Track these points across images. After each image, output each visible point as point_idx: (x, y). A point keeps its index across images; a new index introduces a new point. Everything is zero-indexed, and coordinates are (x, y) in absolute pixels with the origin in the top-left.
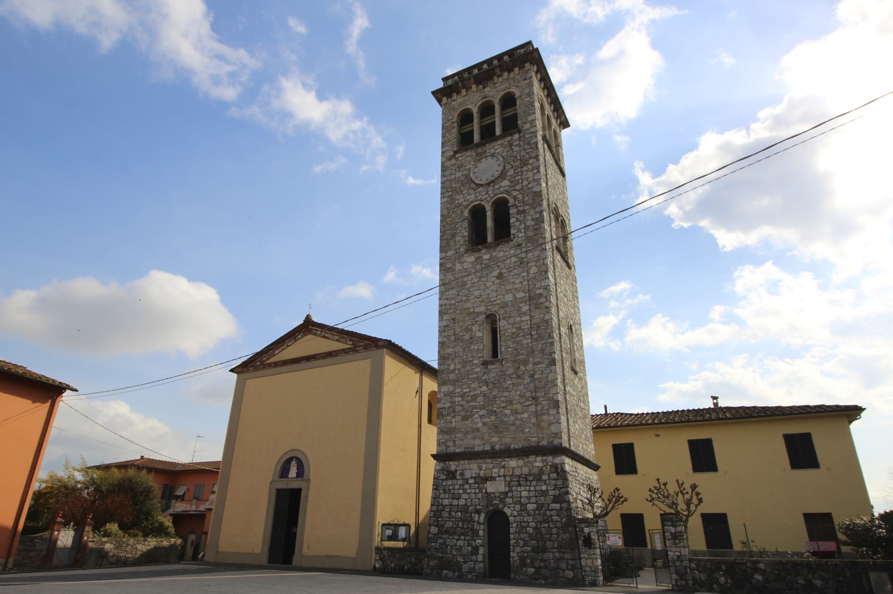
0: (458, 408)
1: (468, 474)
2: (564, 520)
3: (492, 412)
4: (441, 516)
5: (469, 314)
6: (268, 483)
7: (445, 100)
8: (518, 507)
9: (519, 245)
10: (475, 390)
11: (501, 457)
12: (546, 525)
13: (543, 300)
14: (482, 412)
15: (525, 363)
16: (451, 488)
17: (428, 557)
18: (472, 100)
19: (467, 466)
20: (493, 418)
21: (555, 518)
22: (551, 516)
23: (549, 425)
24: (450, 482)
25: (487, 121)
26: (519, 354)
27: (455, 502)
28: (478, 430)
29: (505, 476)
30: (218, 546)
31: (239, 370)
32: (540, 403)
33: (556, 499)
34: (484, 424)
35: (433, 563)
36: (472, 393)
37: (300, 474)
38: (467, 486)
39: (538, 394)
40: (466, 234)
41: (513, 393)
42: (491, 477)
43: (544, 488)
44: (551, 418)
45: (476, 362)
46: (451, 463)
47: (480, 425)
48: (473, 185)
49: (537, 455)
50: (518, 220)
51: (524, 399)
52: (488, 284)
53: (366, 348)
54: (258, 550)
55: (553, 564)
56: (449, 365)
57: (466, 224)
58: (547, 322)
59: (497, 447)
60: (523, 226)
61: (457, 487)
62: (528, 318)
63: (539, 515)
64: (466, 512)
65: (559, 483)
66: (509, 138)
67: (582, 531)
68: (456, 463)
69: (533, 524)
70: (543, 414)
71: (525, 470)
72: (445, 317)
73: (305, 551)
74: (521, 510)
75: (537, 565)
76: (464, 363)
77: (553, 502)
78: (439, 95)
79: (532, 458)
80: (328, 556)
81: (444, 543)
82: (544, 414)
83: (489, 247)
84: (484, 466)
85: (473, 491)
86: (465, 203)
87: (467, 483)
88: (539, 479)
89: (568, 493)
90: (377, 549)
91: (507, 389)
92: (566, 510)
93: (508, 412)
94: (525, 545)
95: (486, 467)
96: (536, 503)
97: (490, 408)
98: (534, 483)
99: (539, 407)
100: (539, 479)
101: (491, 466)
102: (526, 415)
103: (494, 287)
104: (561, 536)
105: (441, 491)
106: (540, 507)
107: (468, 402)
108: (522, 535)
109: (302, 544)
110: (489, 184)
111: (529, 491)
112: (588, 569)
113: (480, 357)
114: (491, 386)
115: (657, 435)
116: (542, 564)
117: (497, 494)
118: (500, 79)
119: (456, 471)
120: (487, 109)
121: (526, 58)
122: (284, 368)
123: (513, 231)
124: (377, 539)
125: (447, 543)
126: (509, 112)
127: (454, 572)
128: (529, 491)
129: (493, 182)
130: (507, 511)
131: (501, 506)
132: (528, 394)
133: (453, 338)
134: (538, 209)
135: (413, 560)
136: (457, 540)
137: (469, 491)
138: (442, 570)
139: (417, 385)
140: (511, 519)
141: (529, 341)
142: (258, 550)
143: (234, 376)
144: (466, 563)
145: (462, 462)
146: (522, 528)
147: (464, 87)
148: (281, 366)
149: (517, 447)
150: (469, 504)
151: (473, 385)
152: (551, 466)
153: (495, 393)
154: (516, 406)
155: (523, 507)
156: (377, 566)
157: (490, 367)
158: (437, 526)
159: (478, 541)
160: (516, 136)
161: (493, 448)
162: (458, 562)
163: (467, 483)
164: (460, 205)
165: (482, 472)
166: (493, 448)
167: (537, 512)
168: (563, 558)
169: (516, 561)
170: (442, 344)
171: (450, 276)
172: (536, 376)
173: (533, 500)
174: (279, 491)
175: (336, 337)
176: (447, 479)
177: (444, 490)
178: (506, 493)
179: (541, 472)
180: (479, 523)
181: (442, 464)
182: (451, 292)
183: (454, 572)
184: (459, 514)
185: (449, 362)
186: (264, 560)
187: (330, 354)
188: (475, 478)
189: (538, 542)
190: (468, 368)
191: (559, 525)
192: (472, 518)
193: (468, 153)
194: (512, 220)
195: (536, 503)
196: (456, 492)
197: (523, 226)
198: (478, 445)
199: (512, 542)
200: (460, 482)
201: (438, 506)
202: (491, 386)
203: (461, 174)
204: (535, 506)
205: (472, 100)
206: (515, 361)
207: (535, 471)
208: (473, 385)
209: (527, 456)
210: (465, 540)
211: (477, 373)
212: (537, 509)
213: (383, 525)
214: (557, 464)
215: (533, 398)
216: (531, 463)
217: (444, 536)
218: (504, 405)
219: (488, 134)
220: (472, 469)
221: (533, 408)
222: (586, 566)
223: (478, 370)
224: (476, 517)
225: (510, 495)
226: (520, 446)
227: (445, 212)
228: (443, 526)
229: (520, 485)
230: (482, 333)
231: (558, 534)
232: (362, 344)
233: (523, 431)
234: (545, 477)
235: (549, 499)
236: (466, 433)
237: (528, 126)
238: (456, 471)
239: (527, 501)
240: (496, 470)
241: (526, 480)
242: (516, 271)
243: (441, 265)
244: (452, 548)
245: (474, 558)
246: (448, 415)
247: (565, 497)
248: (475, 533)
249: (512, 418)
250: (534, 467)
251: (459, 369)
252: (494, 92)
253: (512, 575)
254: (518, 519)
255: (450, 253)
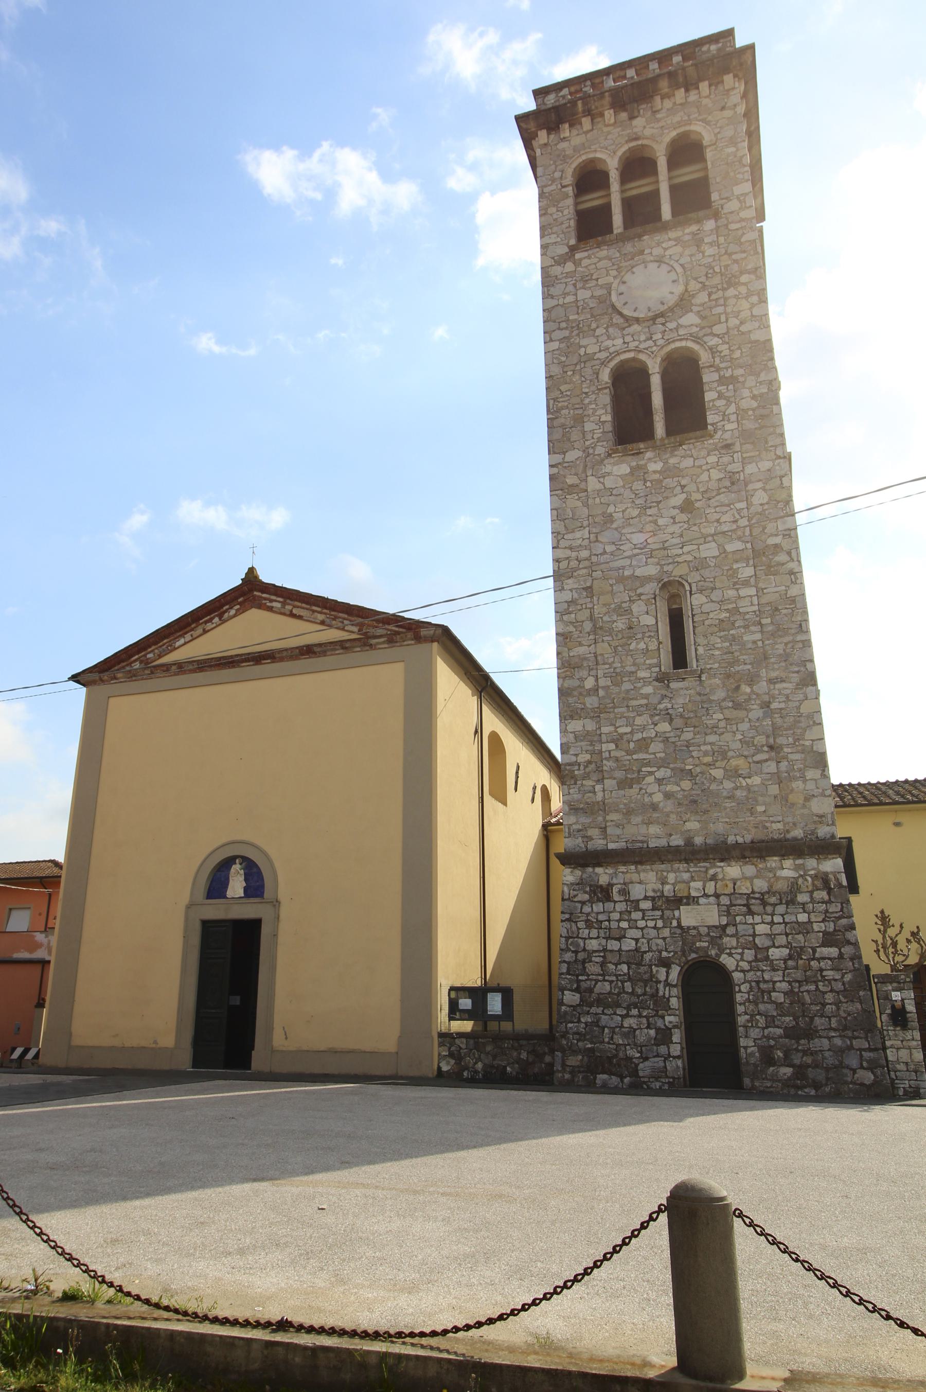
0: (608, 765)
1: (637, 892)
2: (848, 977)
3: (682, 773)
4: (584, 972)
5: (621, 580)
6: (183, 909)
7: (543, 136)
8: (749, 954)
9: (728, 446)
10: (644, 728)
11: (705, 860)
12: (813, 987)
13: (782, 557)
14: (661, 773)
15: (752, 680)
16: (601, 917)
17: (563, 1051)
18: (604, 141)
19: (635, 877)
20: (686, 784)
21: (829, 974)
22: (821, 970)
23: (807, 799)
24: (598, 907)
25: (639, 187)
26: (736, 661)
27: (613, 945)
28: (654, 807)
29: (717, 896)
30: (71, 1034)
31: (96, 676)
32: (785, 758)
33: (829, 940)
34: (668, 796)
35: (574, 1061)
36: (638, 736)
37: (256, 886)
38: (636, 915)
39: (781, 741)
40: (608, 418)
41: (727, 737)
42: (688, 897)
43: (803, 918)
44: (811, 786)
45: (641, 674)
46: (599, 870)
47: (658, 798)
48: (617, 319)
49: (783, 856)
50: (720, 396)
51: (752, 750)
52: (661, 522)
53: (391, 640)
54: (168, 1041)
55: (830, 1059)
56: (582, 680)
57: (605, 398)
58: (793, 600)
59: (698, 840)
60: (732, 409)
61: (616, 916)
62: (753, 591)
63: (796, 968)
64: (639, 964)
65: (834, 908)
66: (694, 228)
67: (887, 997)
68: (610, 871)
69: (784, 986)
70: (791, 779)
71: (761, 885)
72: (570, 583)
73: (278, 1041)
74: (756, 960)
75: (797, 1061)
76: (617, 677)
77: (823, 945)
78: (532, 126)
79: (773, 862)
80: (334, 1052)
81: (596, 1023)
82: (795, 779)
83: (660, 448)
84: (671, 877)
85: (651, 924)
86: (603, 355)
87: (637, 909)
88: (791, 902)
89: (852, 927)
90: (442, 1035)
91: (714, 729)
92: (852, 959)
93: (718, 773)
94: (771, 1022)
95: (676, 878)
96: (788, 945)
97: (679, 765)
98: (781, 909)
99: (784, 765)
100: (791, 902)
101: (686, 876)
102: (756, 780)
103: (676, 529)
104: (844, 1007)
105: (581, 925)
106: (796, 953)
107: (629, 752)
108: (762, 1007)
109: (270, 1029)
110: (654, 319)
111: (772, 923)
112: (902, 1067)
113: (650, 667)
114: (678, 722)
115: (897, 824)
116: (808, 1060)
117: (704, 931)
118: (668, 104)
119: (611, 885)
120: (638, 165)
121: (717, 65)
122: (200, 676)
123: (711, 418)
124: (443, 1014)
125: (602, 1023)
126: (688, 174)
127: (622, 1077)
128: (772, 923)
129: (662, 315)
130: (728, 962)
131: (713, 952)
132: (761, 740)
133: (588, 626)
134: (763, 376)
135: (524, 1055)
136: (623, 1017)
137: (641, 924)
138: (595, 1073)
139: (475, 720)
140: (737, 976)
141: (758, 636)
142: (168, 1041)
143: (80, 692)
144: (646, 1059)
145: (622, 869)
146: (761, 992)
147: (588, 112)
148: (194, 671)
149: (740, 840)
150: (644, 948)
151: (639, 721)
152: (815, 877)
153: (688, 735)
154: (734, 762)
155: (761, 955)
156: (445, 1068)
157: (673, 685)
158: (577, 990)
159: (667, 1018)
160: (710, 225)
161: (689, 842)
162: (629, 1059)
163: (637, 909)
164: (590, 358)
165: (667, 888)
166: (689, 842)
167: (790, 963)
168: (851, 1048)
169: (752, 1054)
170: (563, 639)
171: (573, 501)
172: (774, 705)
173: (782, 940)
174: (207, 925)
175: (321, 617)
176: (591, 901)
177: (587, 921)
178: (724, 928)
179: (794, 888)
180: (667, 984)
181: (578, 873)
182: (578, 534)
183: (622, 1077)
184: (624, 968)
185: (584, 673)
186: (184, 1060)
187: (308, 651)
188: (653, 899)
189: (796, 1019)
190: (626, 686)
191: (839, 986)
192: (652, 976)
193: (603, 253)
194: (709, 396)
195: (788, 945)
196: (614, 925)
197: (732, 409)
198: (655, 835)
199: (741, 1020)
200: (621, 907)
201: (576, 952)
202: (678, 722)
203: (587, 294)
204: (786, 951)
205: (604, 141)
206: (728, 676)
207: (781, 886)
208: (639, 721)
209: (762, 857)
210: (640, 1016)
211: (646, 696)
212: (790, 957)
213: (452, 989)
214: (826, 874)
215: (771, 748)
216: (771, 870)
217: (593, 1010)
218: (709, 759)
219: (642, 214)
220: (645, 881)
221: (771, 767)
222: (898, 1062)
223: (648, 690)
224: (662, 973)
225: (730, 930)
226: (748, 838)
227: (556, 370)
228: (590, 990)
229: (751, 913)
230: (652, 618)
231: (837, 1004)
232: (380, 632)
233: (752, 811)
234: (802, 898)
235: (815, 940)
236: (629, 813)
237: (733, 205)
238: (611, 885)
239: (768, 943)
240: (699, 884)
241: (764, 904)
242: (722, 498)
243: (552, 478)
244: (612, 1030)
245: (663, 1049)
246: (586, 776)
247: (849, 936)
248: (662, 1004)
249: (728, 785)
250: (778, 879)
251: (606, 688)
252: (656, 129)
253: (747, 1081)
254: (750, 976)
255: (572, 456)
